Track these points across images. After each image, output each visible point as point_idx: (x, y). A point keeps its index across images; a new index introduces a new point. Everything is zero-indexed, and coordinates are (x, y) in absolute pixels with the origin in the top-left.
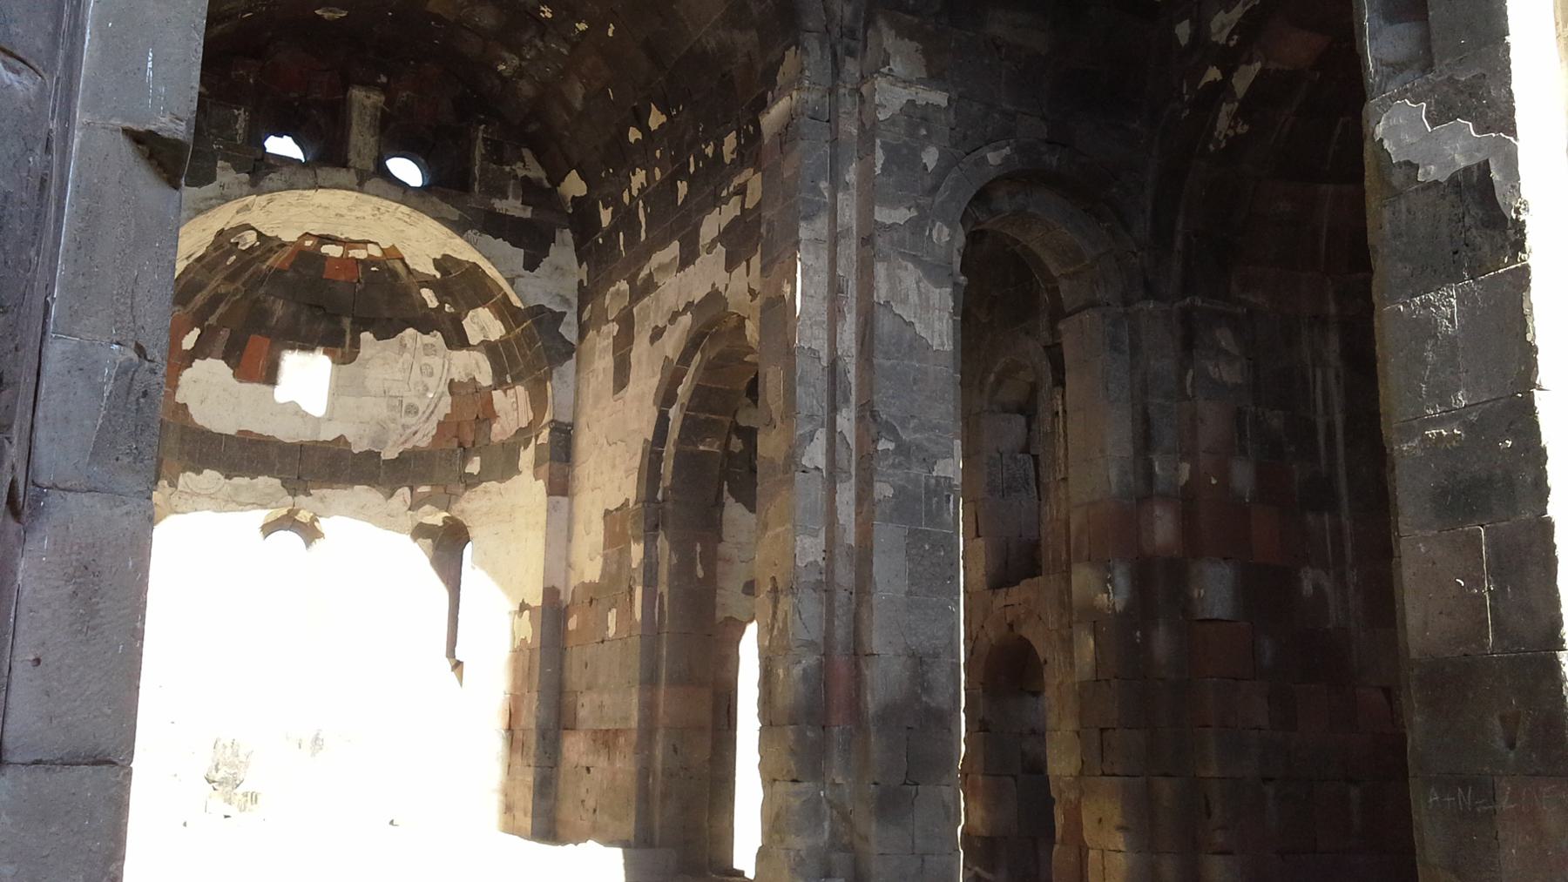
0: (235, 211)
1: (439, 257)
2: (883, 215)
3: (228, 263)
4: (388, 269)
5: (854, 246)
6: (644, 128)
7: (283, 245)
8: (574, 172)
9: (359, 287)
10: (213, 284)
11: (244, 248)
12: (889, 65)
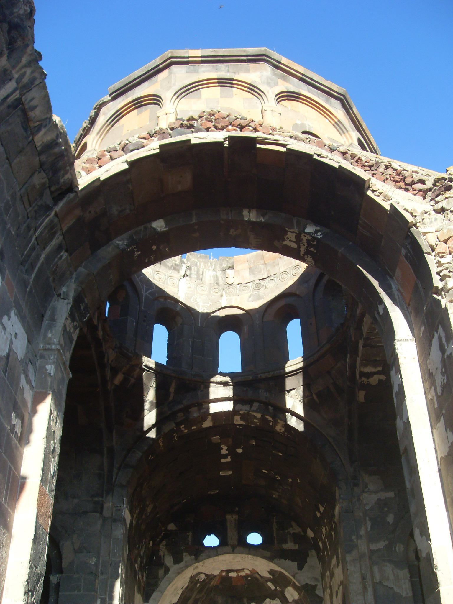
0: (193, 570)
1: (269, 570)
2: (374, 547)
3: (197, 587)
4: (254, 577)
5: (367, 560)
6: (320, 512)
7: (215, 576)
8: (309, 530)
9: (246, 586)
10: (193, 597)
11: (202, 580)
12: (367, 487)
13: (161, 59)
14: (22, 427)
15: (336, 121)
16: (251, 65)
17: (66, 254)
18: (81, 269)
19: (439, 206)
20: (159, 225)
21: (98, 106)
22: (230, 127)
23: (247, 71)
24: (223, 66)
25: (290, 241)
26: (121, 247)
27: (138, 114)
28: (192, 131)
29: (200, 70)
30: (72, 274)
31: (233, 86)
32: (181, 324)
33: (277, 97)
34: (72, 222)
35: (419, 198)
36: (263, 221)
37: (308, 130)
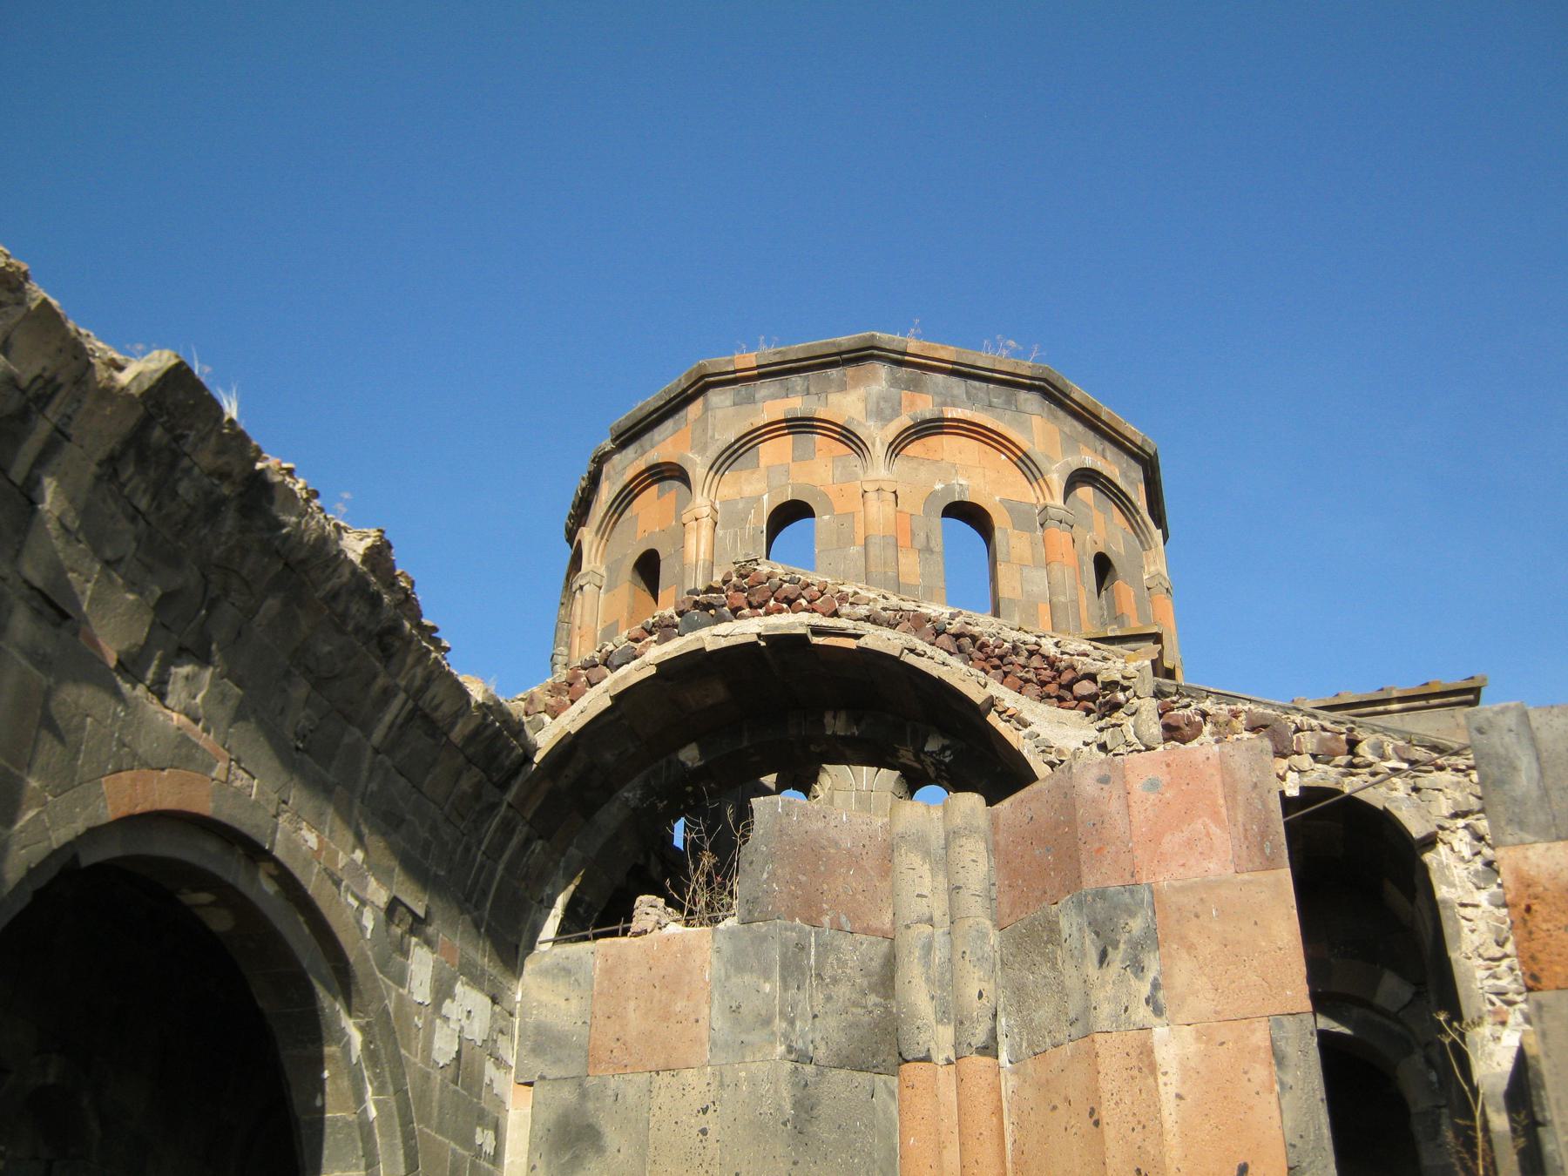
13: (689, 375)
14: (496, 1139)
15: (1020, 454)
16: (850, 371)
17: (540, 842)
18: (572, 851)
19: (1106, 737)
20: (690, 755)
21: (597, 460)
22: (772, 602)
23: (843, 387)
24: (798, 379)
25: (908, 759)
26: (633, 804)
27: (658, 498)
28: (712, 616)
29: (757, 396)
30: (557, 864)
31: (815, 430)
32: (829, 789)
33: (893, 447)
34: (539, 803)
35: (1076, 715)
36: (857, 733)
37: (957, 500)
